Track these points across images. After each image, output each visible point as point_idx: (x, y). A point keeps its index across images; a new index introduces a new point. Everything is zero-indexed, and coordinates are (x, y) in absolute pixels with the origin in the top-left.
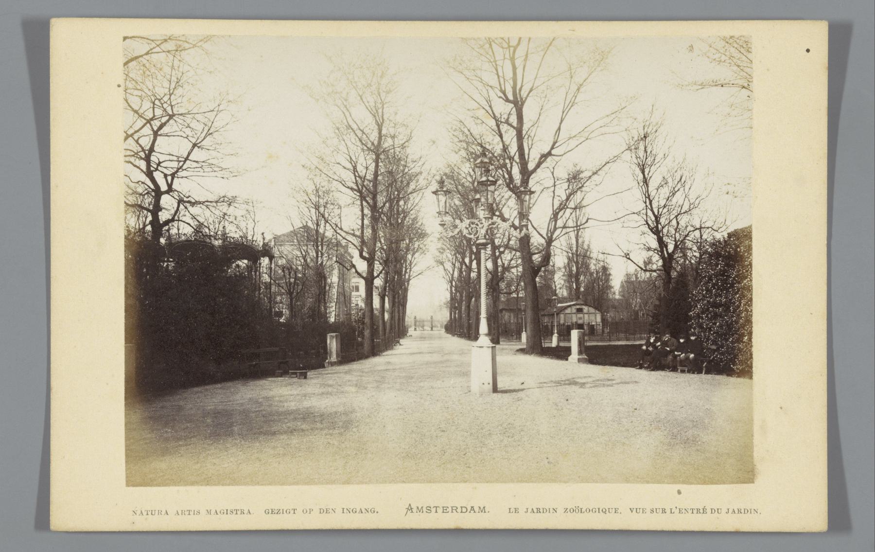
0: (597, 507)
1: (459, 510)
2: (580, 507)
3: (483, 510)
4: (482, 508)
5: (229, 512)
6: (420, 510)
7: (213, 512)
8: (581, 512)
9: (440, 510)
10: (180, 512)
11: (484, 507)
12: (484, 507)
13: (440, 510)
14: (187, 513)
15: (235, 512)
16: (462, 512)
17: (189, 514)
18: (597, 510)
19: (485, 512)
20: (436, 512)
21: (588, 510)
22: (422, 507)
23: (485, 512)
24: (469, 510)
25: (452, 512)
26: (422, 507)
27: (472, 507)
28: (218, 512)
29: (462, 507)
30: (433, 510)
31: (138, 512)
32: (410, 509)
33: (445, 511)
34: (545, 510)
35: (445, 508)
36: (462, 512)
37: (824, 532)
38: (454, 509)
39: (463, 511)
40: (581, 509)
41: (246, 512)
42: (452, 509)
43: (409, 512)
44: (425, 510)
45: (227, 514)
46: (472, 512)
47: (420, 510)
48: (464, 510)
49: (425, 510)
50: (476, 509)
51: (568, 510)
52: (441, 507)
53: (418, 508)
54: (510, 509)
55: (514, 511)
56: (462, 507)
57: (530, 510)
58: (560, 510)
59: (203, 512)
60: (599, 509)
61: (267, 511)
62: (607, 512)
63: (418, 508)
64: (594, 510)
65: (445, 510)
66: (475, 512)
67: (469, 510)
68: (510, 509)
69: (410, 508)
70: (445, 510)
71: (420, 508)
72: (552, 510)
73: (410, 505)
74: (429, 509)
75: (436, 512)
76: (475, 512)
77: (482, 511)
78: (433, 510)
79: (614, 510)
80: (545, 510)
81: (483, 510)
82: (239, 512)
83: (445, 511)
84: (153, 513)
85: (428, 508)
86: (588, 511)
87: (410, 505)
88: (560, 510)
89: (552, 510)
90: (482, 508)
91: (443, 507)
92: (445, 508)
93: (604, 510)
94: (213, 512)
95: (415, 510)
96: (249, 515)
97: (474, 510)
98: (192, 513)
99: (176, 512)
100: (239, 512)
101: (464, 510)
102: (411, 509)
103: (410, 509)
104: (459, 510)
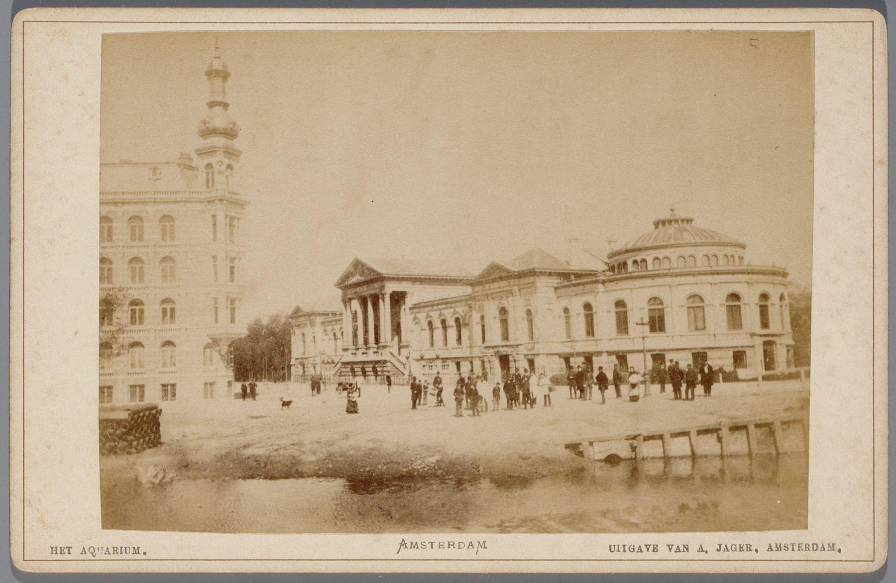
1: (456, 545)
4: (481, 543)
22: (416, 543)
23: (485, 548)
24: (467, 545)
25: (449, 547)
36: (459, 548)
42: (449, 545)
46: (471, 547)
53: (412, 543)
60: (624, 546)
63: (412, 543)
69: (403, 543)
83: (441, 547)
85: (423, 543)
90: (481, 543)
95: (409, 545)
97: (472, 545)
102: (405, 544)
104: (456, 545)
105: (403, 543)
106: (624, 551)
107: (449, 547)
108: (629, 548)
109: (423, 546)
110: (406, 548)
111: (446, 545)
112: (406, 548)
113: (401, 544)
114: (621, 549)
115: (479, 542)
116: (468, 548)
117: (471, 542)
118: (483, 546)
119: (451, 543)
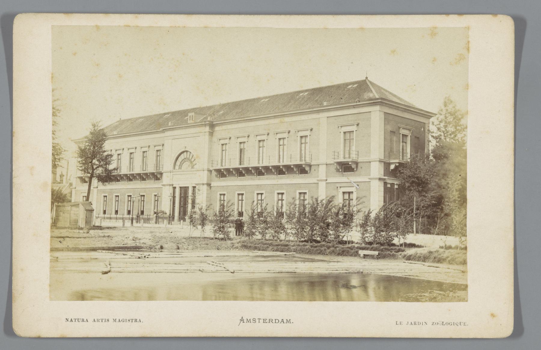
1: (274, 321)
3: (288, 321)
5: (127, 320)
6: (248, 321)
7: (117, 320)
10: (96, 320)
13: (261, 321)
14: (100, 321)
15: (131, 321)
16: (275, 323)
19: (290, 323)
21: (447, 323)
25: (269, 322)
27: (283, 320)
28: (121, 321)
29: (275, 320)
30: (257, 321)
31: (69, 320)
32: (242, 320)
33: (265, 322)
34: (419, 323)
36: (275, 323)
38: (271, 321)
40: (443, 322)
41: (138, 320)
43: (241, 322)
46: (282, 322)
47: (248, 321)
49: (252, 321)
50: (285, 321)
51: (435, 323)
56: (275, 320)
58: (430, 324)
59: (111, 320)
63: (247, 319)
65: (264, 321)
66: (284, 323)
69: (242, 320)
70: (264, 321)
71: (249, 320)
72: (424, 323)
78: (257, 321)
80: (419, 323)
81: (288, 321)
82: (134, 321)
83: (265, 322)
84: (79, 321)
85: (254, 320)
86: (447, 324)
89: (424, 323)
91: (264, 319)
92: (265, 320)
93: (457, 324)
94: (117, 320)
95: (245, 321)
96: (140, 322)
97: (283, 321)
98: (104, 321)
99: (93, 320)
100: (134, 321)
102: (243, 320)
104: (274, 321)
105: (242, 320)
107: (269, 322)
110: (244, 322)
111: (268, 321)
112: (244, 322)
113: (241, 320)
114: (453, 324)
117: (283, 320)
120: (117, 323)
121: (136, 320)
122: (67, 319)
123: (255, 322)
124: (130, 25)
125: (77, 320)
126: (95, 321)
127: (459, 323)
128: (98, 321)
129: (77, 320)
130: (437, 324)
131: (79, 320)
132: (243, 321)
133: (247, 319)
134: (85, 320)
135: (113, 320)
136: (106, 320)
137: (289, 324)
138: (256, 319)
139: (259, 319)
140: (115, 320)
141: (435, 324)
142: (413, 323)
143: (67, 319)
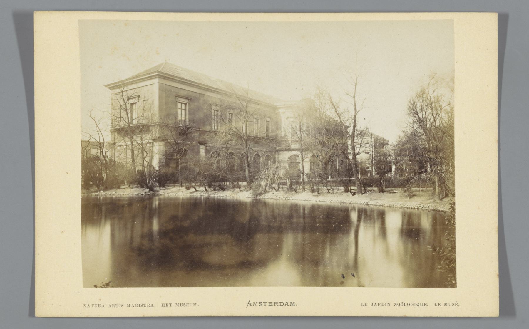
0: (414, 303)
1: (279, 304)
2: (404, 302)
3: (293, 304)
4: (292, 303)
6: (255, 304)
7: (131, 305)
8: (404, 305)
9: (267, 304)
10: (112, 306)
11: (294, 303)
12: (294, 303)
13: (267, 304)
15: (144, 306)
16: (280, 305)
17: (145, 306)
18: (414, 304)
19: (294, 305)
20: (265, 305)
21: (408, 304)
22: (257, 303)
23: (294, 305)
24: (284, 304)
25: (275, 305)
26: (257, 303)
27: (287, 302)
28: (134, 306)
29: (280, 303)
30: (263, 304)
31: (87, 306)
32: (249, 303)
33: (270, 305)
34: (383, 304)
35: (270, 303)
37: (497, 317)
39: (281, 305)
40: (405, 303)
42: (275, 304)
44: (258, 304)
45: (139, 306)
46: (287, 305)
47: (255, 304)
48: (282, 304)
49: (258, 304)
50: (289, 304)
51: (397, 304)
52: (268, 302)
54: (362, 303)
55: (364, 305)
56: (280, 303)
57: (374, 304)
58: (392, 304)
59: (125, 305)
61: (137, 305)
62: (420, 305)
64: (412, 304)
66: (288, 305)
67: (284, 304)
68: (362, 303)
69: (249, 303)
71: (255, 303)
72: (387, 304)
73: (249, 301)
74: (261, 304)
75: (265, 305)
76: (288, 305)
77: (292, 305)
78: (263, 304)
79: (424, 304)
80: (383, 304)
81: (293, 304)
82: (146, 306)
83: (270, 305)
87: (249, 301)
88: (392, 304)
89: (387, 304)
90: (292, 303)
91: (269, 302)
92: (270, 303)
95: (252, 304)
96: (152, 307)
97: (287, 304)
98: (118, 306)
99: (109, 305)
101: (281, 304)
102: (250, 303)
103: (249, 303)
104: (279, 304)
105: (249, 303)
106: (415, 305)
107: (275, 305)
108: (417, 304)
109: (260, 305)
110: (251, 305)
111: (273, 304)
112: (251, 305)
113: (248, 303)
115: (291, 303)
116: (285, 305)
117: (287, 302)
118: (293, 305)
119: (276, 303)
120: (131, 308)
121: (148, 305)
122: (84, 305)
123: (261, 305)
124: (455, 83)
125: (94, 306)
126: (376, 305)
127: (420, 304)
128: (114, 306)
129: (94, 306)
130: (399, 305)
131: (96, 305)
132: (250, 304)
133: (254, 303)
134: (101, 305)
135: (127, 305)
136: (121, 306)
137: (293, 306)
138: (262, 303)
139: (265, 302)
140: (129, 306)
141: (397, 305)
142: (377, 304)
143: (84, 305)
